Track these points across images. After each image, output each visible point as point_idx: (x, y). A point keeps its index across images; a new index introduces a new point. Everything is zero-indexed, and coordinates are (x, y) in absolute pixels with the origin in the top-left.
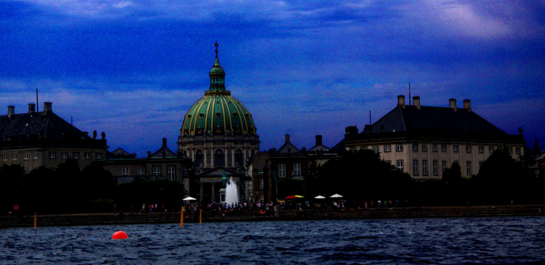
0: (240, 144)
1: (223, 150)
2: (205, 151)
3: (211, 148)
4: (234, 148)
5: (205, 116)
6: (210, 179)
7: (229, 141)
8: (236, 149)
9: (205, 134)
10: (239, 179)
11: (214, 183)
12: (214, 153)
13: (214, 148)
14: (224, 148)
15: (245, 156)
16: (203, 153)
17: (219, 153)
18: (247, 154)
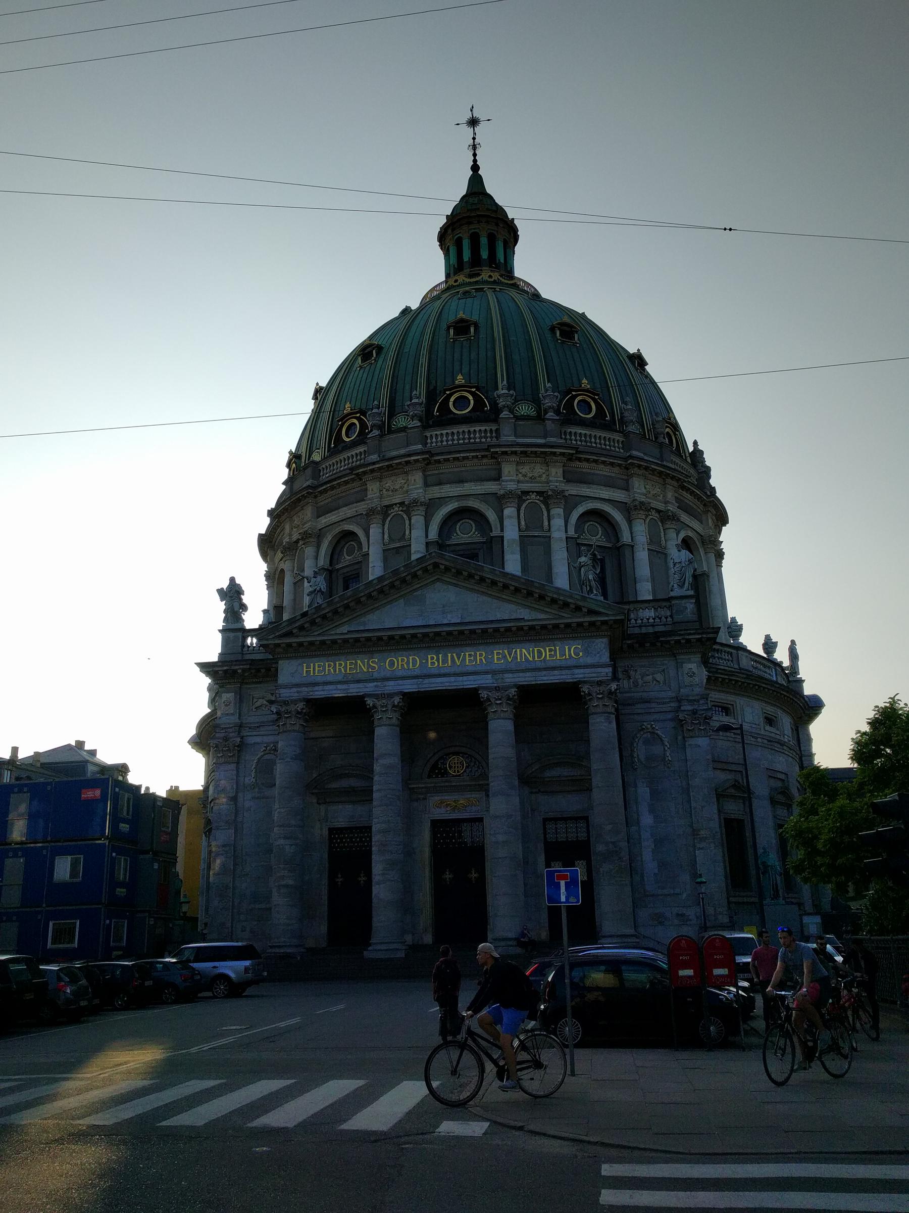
0: (609, 483)
1: (491, 515)
2: (374, 531)
3: (408, 508)
4: (570, 503)
5: (385, 350)
6: (362, 665)
7: (526, 454)
8: (581, 509)
9: (380, 427)
10: (605, 658)
11: (390, 696)
12: (433, 534)
13: (430, 507)
14: (499, 501)
15: (642, 556)
16: (365, 550)
17: (466, 534)
18: (658, 553)
